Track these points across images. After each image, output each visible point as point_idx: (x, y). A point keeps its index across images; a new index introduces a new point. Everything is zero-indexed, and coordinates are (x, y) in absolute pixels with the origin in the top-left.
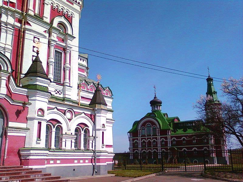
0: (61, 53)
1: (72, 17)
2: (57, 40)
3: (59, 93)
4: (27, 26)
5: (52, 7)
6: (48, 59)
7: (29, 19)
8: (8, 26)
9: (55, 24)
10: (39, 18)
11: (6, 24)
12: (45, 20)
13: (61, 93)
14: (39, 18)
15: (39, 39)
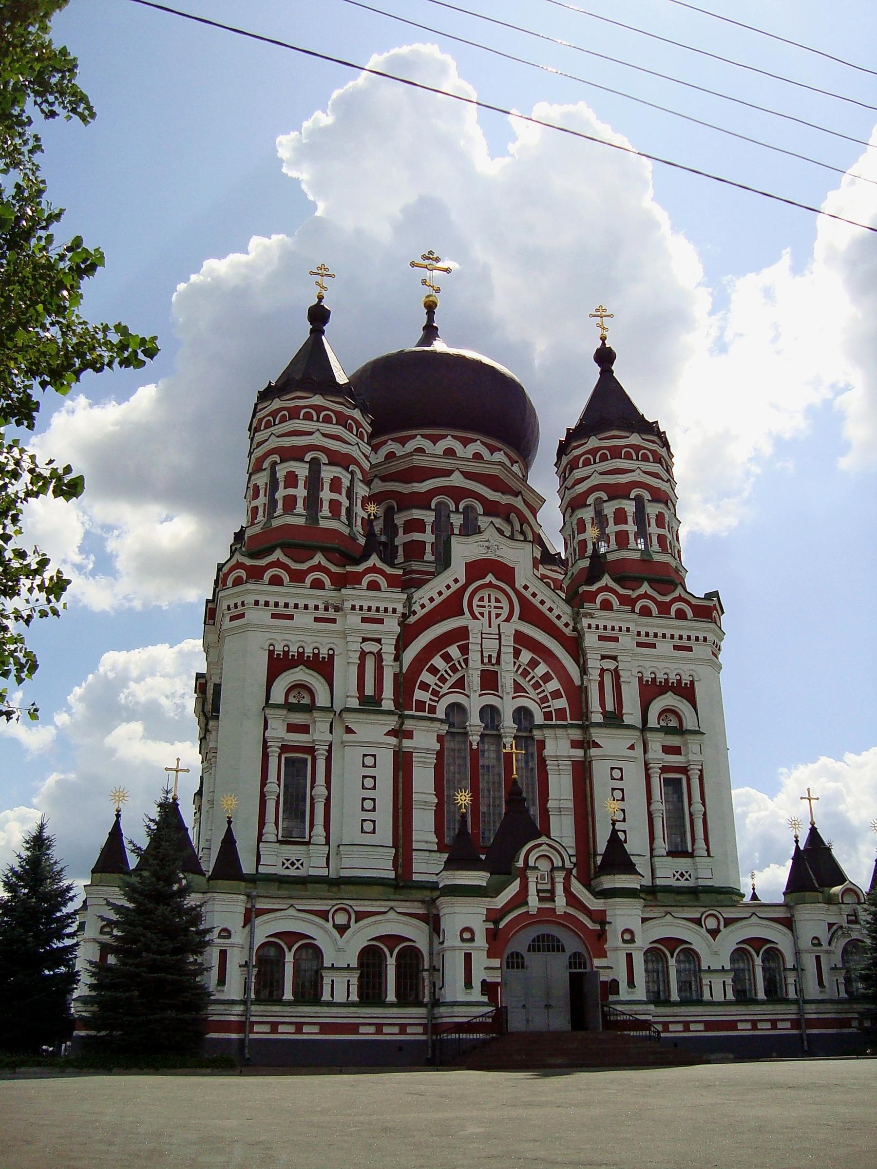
0: (680, 779)
1: (692, 682)
2: (664, 756)
3: (684, 878)
4: (593, 751)
5: (640, 679)
6: (649, 803)
7: (597, 734)
8: (560, 762)
9: (653, 722)
10: (614, 720)
11: (557, 758)
12: (627, 720)
13: (690, 876)
14: (614, 720)
15: (621, 769)
